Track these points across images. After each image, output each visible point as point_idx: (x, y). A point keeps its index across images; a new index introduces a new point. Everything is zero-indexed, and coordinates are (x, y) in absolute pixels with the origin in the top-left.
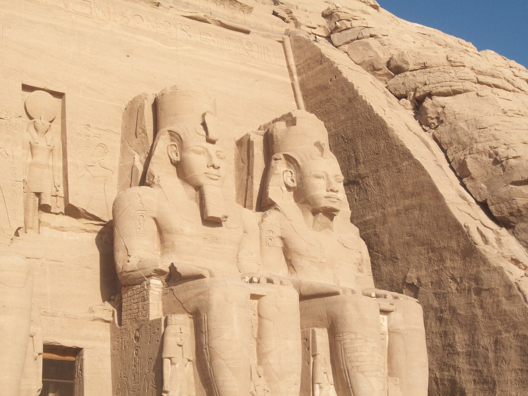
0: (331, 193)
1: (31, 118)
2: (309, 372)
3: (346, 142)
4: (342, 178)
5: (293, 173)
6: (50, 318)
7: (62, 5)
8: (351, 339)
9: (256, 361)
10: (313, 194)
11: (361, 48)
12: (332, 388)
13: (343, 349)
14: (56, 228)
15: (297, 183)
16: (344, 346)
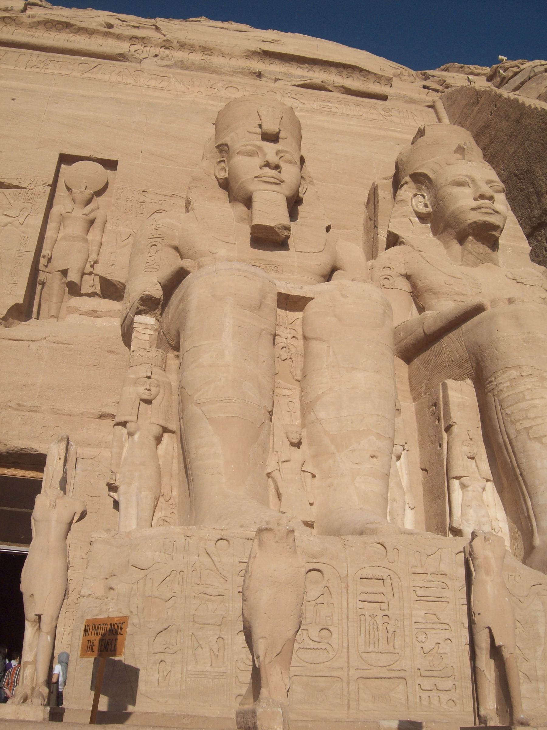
0: (481, 202)
1: (69, 189)
2: (442, 460)
3: (521, 179)
4: (502, 185)
5: (426, 195)
6: (27, 413)
7: (128, 81)
8: (511, 380)
9: (298, 422)
10: (453, 208)
11: (534, 84)
12: (491, 487)
13: (497, 403)
14: (87, 314)
15: (432, 206)
16: (498, 397)
